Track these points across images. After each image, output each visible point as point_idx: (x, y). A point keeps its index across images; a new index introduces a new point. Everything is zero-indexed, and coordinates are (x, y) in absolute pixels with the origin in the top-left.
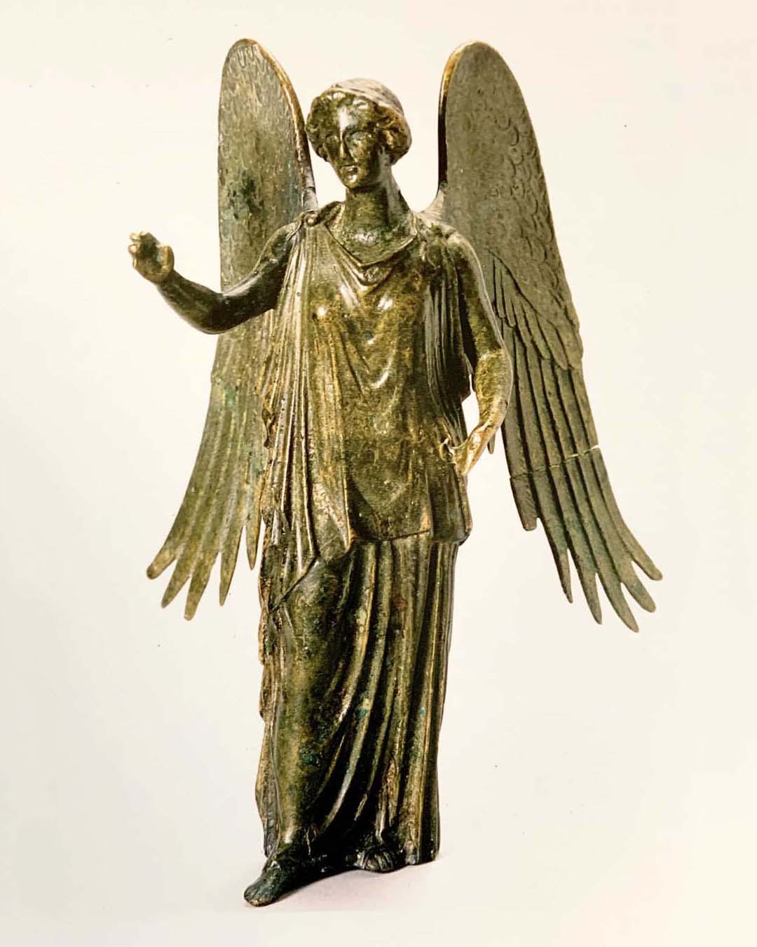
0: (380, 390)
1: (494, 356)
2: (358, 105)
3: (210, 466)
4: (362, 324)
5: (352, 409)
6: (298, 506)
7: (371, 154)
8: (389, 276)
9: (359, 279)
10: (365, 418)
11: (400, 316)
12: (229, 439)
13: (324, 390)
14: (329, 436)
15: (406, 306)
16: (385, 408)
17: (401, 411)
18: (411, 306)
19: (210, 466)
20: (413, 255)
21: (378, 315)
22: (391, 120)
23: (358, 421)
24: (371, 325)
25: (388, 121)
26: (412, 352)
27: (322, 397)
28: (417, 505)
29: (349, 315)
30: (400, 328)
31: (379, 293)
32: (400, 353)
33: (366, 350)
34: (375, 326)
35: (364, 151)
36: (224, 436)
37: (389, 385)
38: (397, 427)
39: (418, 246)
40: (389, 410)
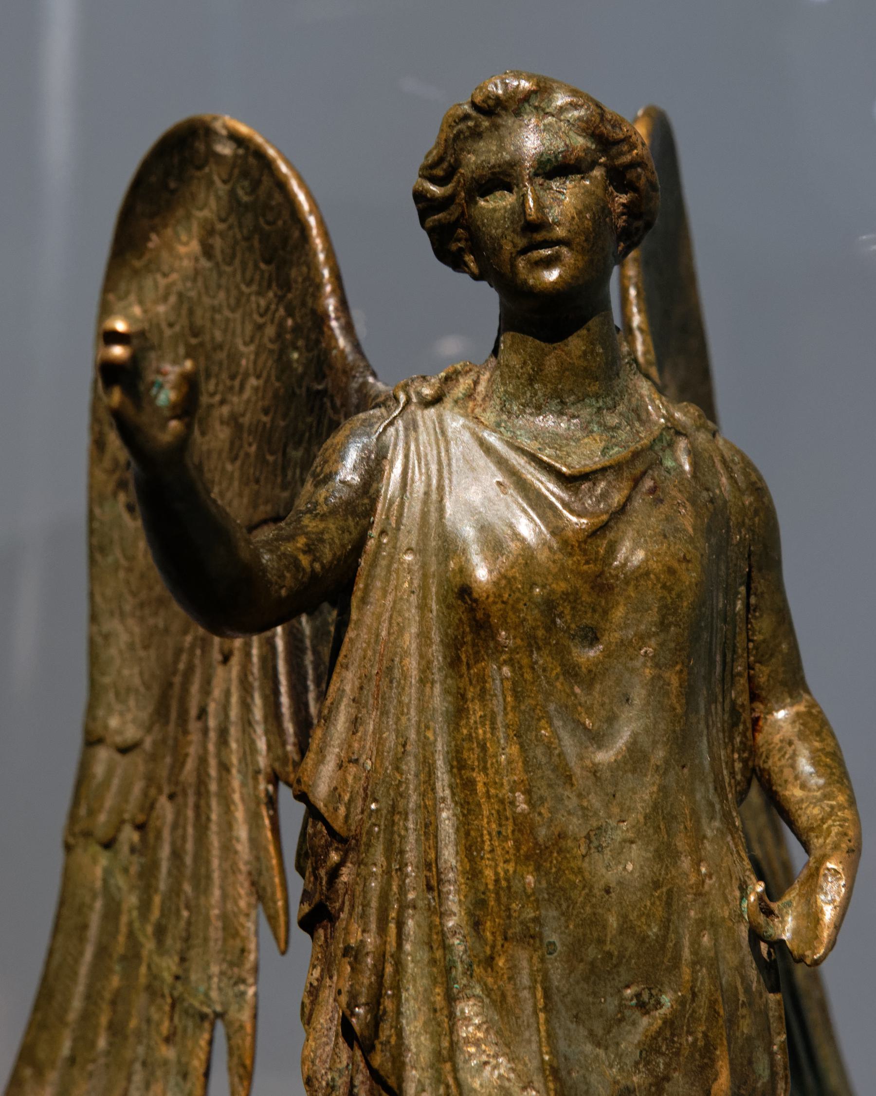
0: (616, 767)
1: (801, 708)
2: (562, 109)
3: (72, 1016)
4: (573, 608)
5: (553, 811)
6: (425, 1057)
7: (593, 219)
8: (629, 499)
9: (565, 505)
10: (584, 833)
11: (664, 587)
12: (115, 956)
13: (485, 769)
14: (497, 881)
15: (676, 565)
16: (629, 809)
17: (661, 816)
18: (684, 565)
19: (72, 1016)
20: (669, 463)
21: (611, 588)
22: (633, 146)
23: (570, 843)
24: (594, 611)
25: (625, 148)
26: (685, 675)
27: (480, 788)
28: (701, 1043)
29: (543, 587)
30: (664, 617)
31: (611, 535)
32: (660, 677)
33: (584, 670)
34: (605, 612)
35: (579, 213)
36: (103, 952)
37: (635, 758)
38: (658, 856)
39: (671, 445)
40: (636, 816)
